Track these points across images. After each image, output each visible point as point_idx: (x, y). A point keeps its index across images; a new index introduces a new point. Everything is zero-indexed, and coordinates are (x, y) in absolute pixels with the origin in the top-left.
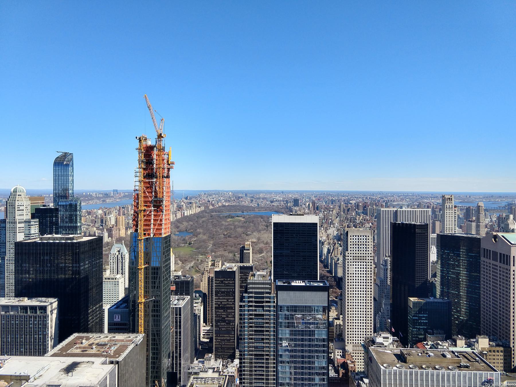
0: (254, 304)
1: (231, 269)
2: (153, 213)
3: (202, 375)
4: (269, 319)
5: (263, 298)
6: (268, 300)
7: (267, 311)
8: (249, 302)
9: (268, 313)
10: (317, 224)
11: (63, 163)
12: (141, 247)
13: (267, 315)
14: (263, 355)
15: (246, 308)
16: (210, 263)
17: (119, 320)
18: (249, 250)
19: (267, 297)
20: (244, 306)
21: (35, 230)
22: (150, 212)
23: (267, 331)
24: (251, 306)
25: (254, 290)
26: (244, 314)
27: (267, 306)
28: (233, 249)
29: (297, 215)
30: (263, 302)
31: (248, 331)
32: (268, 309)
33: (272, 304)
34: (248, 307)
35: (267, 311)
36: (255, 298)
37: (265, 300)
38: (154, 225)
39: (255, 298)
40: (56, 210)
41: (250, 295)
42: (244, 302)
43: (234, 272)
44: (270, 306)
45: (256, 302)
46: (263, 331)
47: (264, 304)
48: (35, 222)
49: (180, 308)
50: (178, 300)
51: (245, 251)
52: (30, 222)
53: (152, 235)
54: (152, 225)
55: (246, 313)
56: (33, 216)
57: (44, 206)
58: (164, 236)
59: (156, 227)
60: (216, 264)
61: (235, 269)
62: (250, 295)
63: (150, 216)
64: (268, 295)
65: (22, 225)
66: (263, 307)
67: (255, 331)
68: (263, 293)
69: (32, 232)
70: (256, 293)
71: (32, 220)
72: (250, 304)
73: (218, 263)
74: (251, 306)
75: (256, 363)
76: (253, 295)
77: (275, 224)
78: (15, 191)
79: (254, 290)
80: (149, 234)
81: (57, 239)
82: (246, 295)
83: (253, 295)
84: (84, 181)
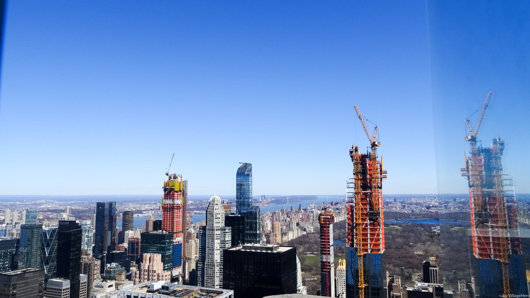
1: (426, 289)
2: (369, 227)
11: (244, 173)
12: (361, 262)
16: (388, 280)
21: (228, 238)
22: (367, 225)
28: (398, 262)
38: (372, 240)
40: (242, 218)
48: (229, 229)
51: (430, 268)
52: (225, 230)
53: (369, 251)
54: (369, 240)
56: (227, 225)
57: (232, 214)
58: (382, 252)
59: (373, 242)
60: (395, 280)
63: (367, 229)
65: (219, 232)
69: (227, 239)
71: (227, 228)
73: (397, 280)
78: (213, 201)
80: (366, 250)
84: (260, 188)
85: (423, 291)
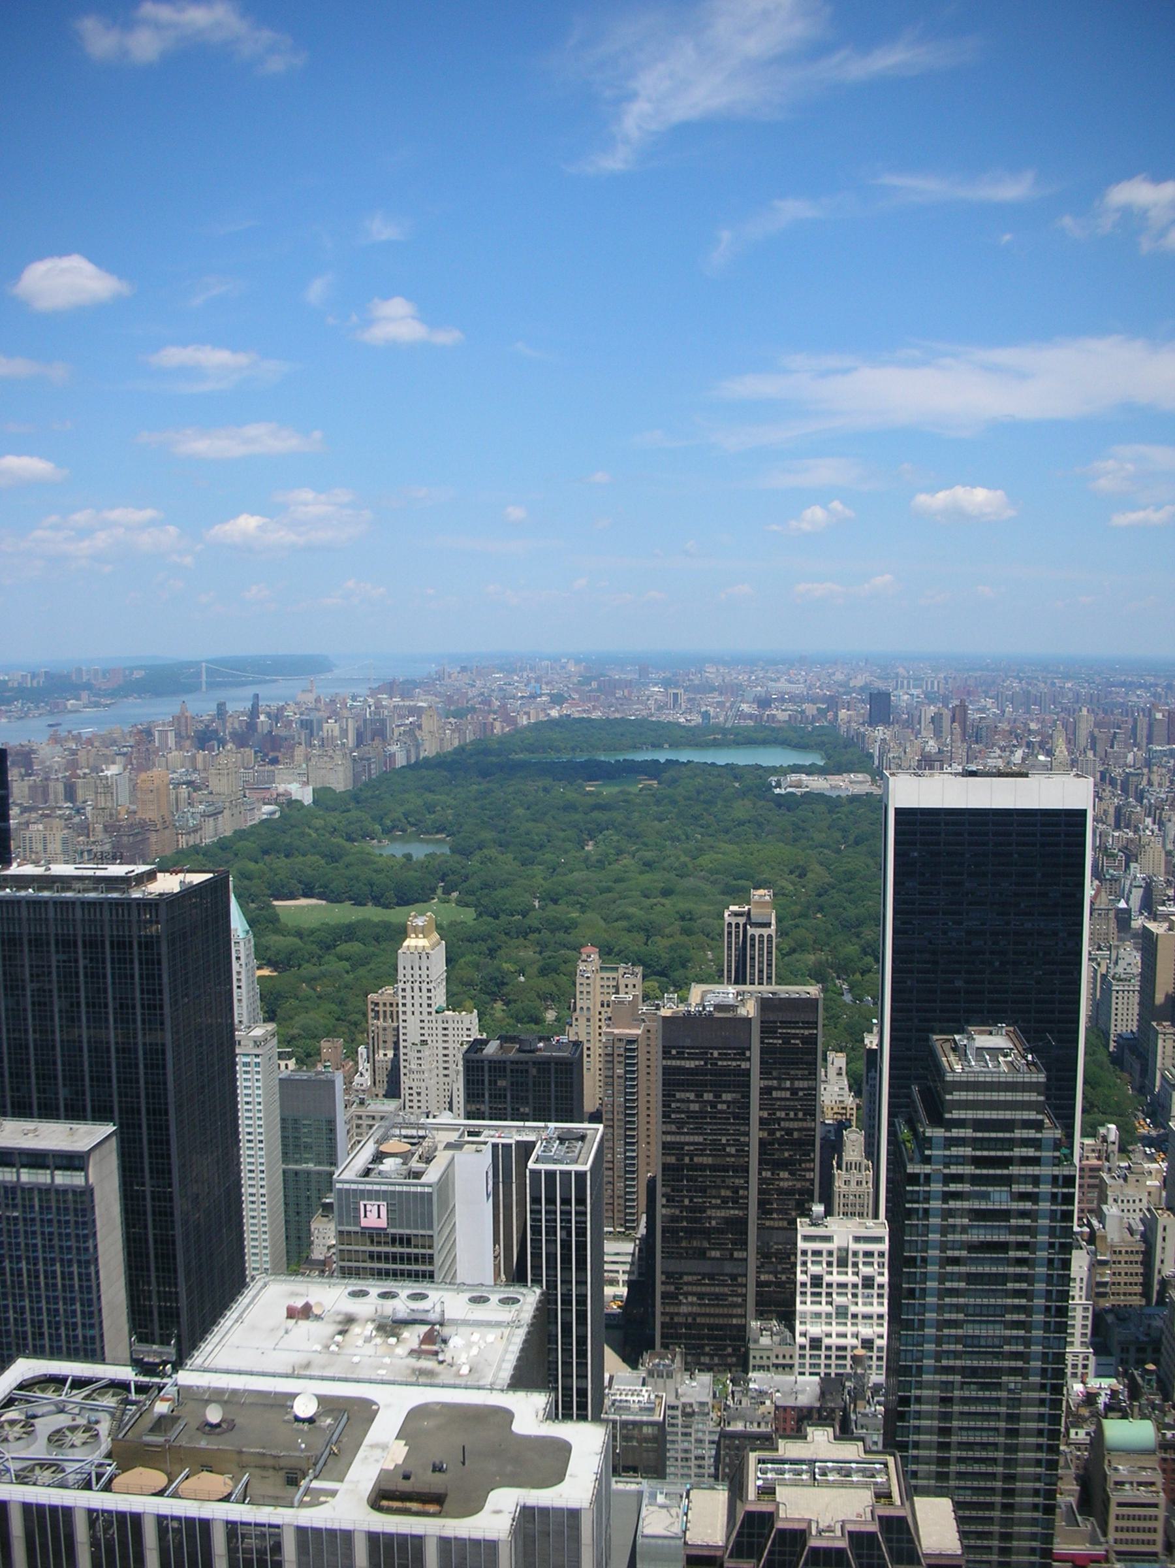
0: (969, 1170)
3: (788, 1449)
4: (1031, 1231)
5: (1011, 1143)
6: (1031, 1152)
7: (1023, 1197)
8: (948, 1161)
9: (1028, 1205)
10: (1082, 813)
13: (1023, 1214)
14: (998, 1372)
15: (936, 1187)
17: (383, 1223)
18: (768, 925)
19: (1026, 1143)
20: (928, 1177)
23: (1019, 1278)
24: (958, 1178)
25: (970, 1115)
26: (926, 1211)
27: (1025, 1179)
29: (1000, 774)
30: (1007, 1162)
31: (942, 1278)
32: (1029, 1188)
33: (1046, 1171)
34: (946, 1184)
35: (1023, 1197)
36: (976, 1143)
37: (1018, 1152)
39: (976, 1143)
41: (955, 1133)
42: (927, 1160)
43: (747, 1021)
44: (1036, 1180)
45: (977, 1162)
46: (1004, 1278)
47: (1014, 1170)
49: (581, 1176)
50: (562, 1140)
51: (751, 931)
55: (935, 1204)
61: (749, 1010)
62: (955, 1133)
64: (1032, 1134)
66: (1008, 1180)
67: (970, 1278)
68: (1008, 1125)
70: (979, 1125)
72: (954, 1170)
74: (958, 1178)
75: (965, 1401)
76: (968, 1133)
77: (899, 812)
79: (970, 1115)
81: (65, 882)
82: (939, 1133)
83: (968, 1133)
85: (717, 1015)
